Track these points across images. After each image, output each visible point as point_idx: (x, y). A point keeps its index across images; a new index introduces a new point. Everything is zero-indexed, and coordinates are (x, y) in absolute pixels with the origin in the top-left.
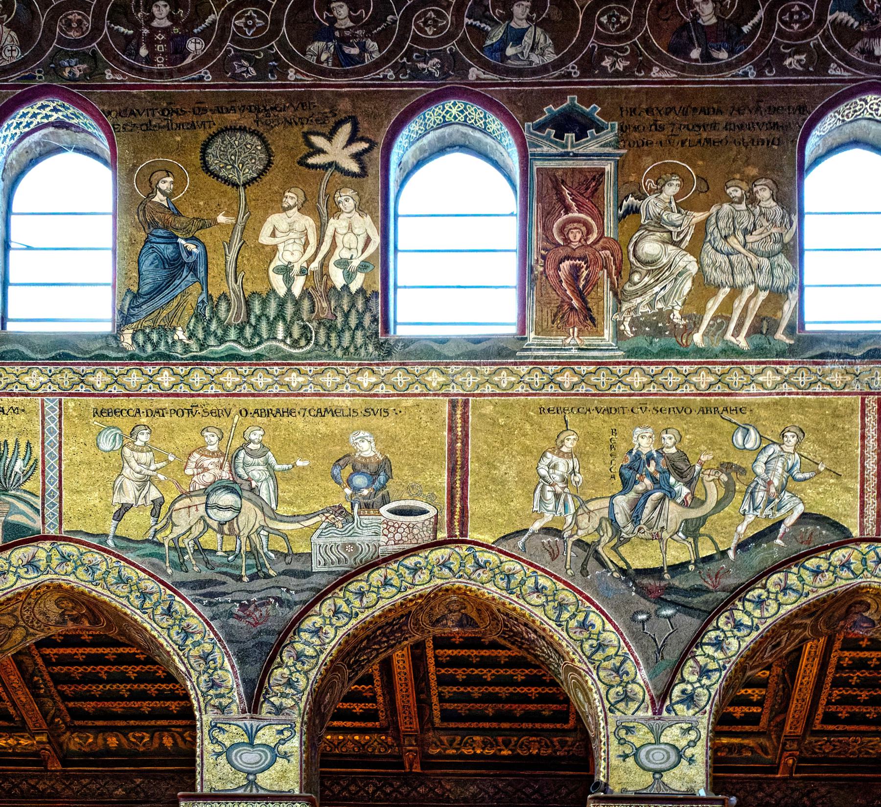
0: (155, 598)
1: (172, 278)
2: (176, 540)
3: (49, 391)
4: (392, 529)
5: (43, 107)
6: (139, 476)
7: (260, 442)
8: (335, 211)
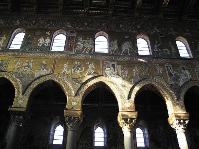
1: (27, 44)
2: (19, 72)
8: (46, 38)
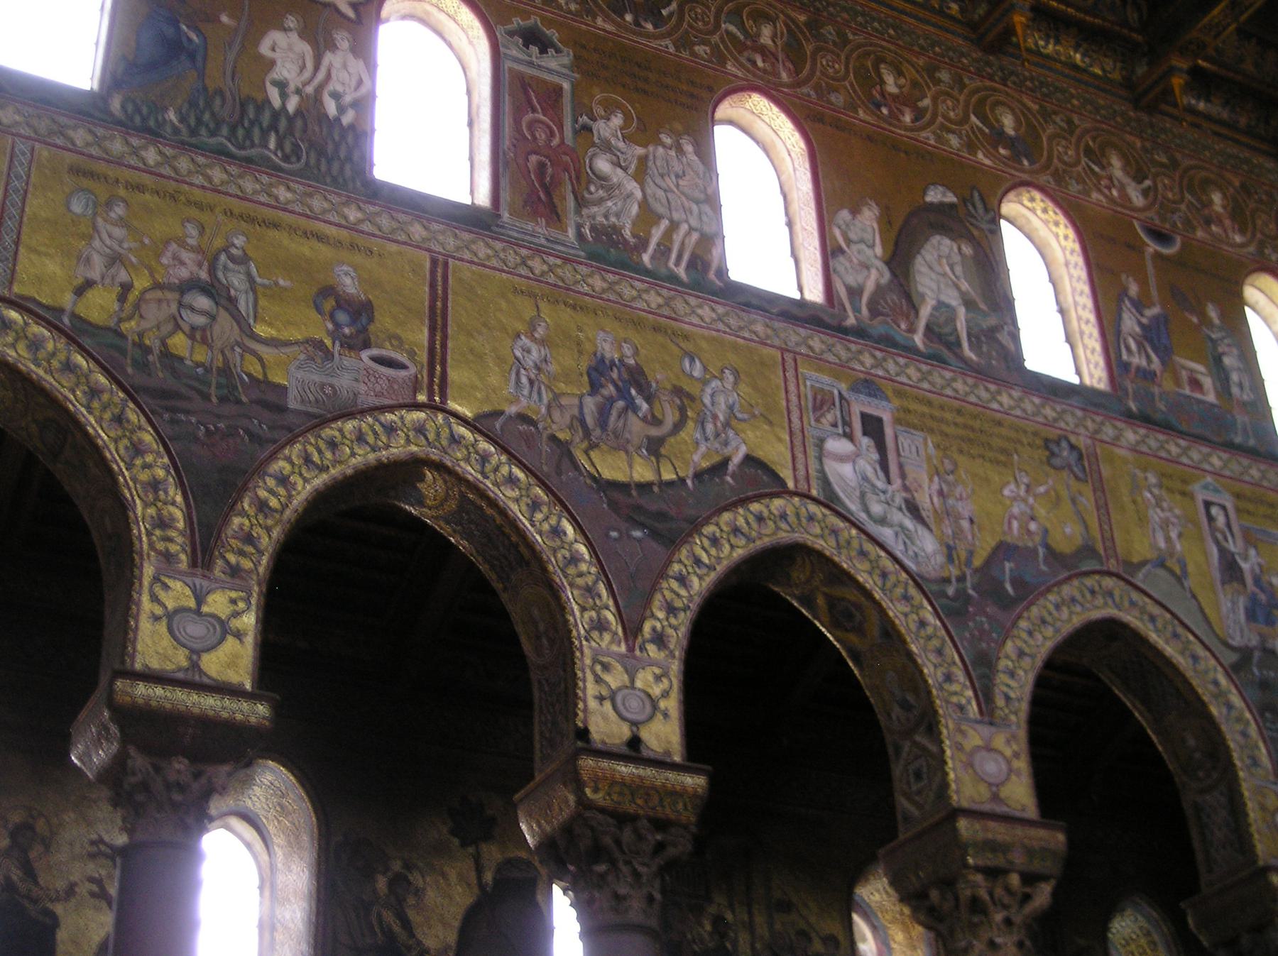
2: (141, 335)
4: (373, 379)
6: (108, 251)
8: (333, 47)
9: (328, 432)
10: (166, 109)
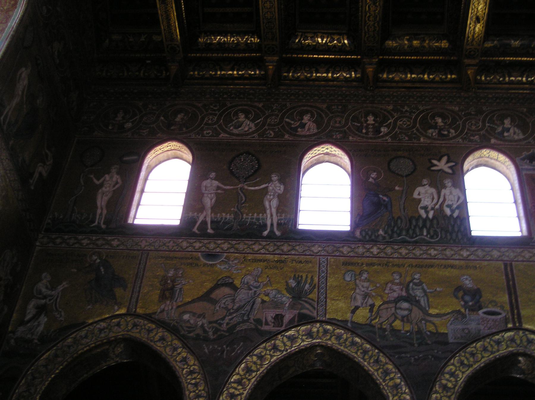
0: (370, 353)
2: (381, 324)
3: (322, 254)
5: (323, 148)
7: (419, 279)
8: (445, 187)
9: (469, 350)
10: (378, 230)
